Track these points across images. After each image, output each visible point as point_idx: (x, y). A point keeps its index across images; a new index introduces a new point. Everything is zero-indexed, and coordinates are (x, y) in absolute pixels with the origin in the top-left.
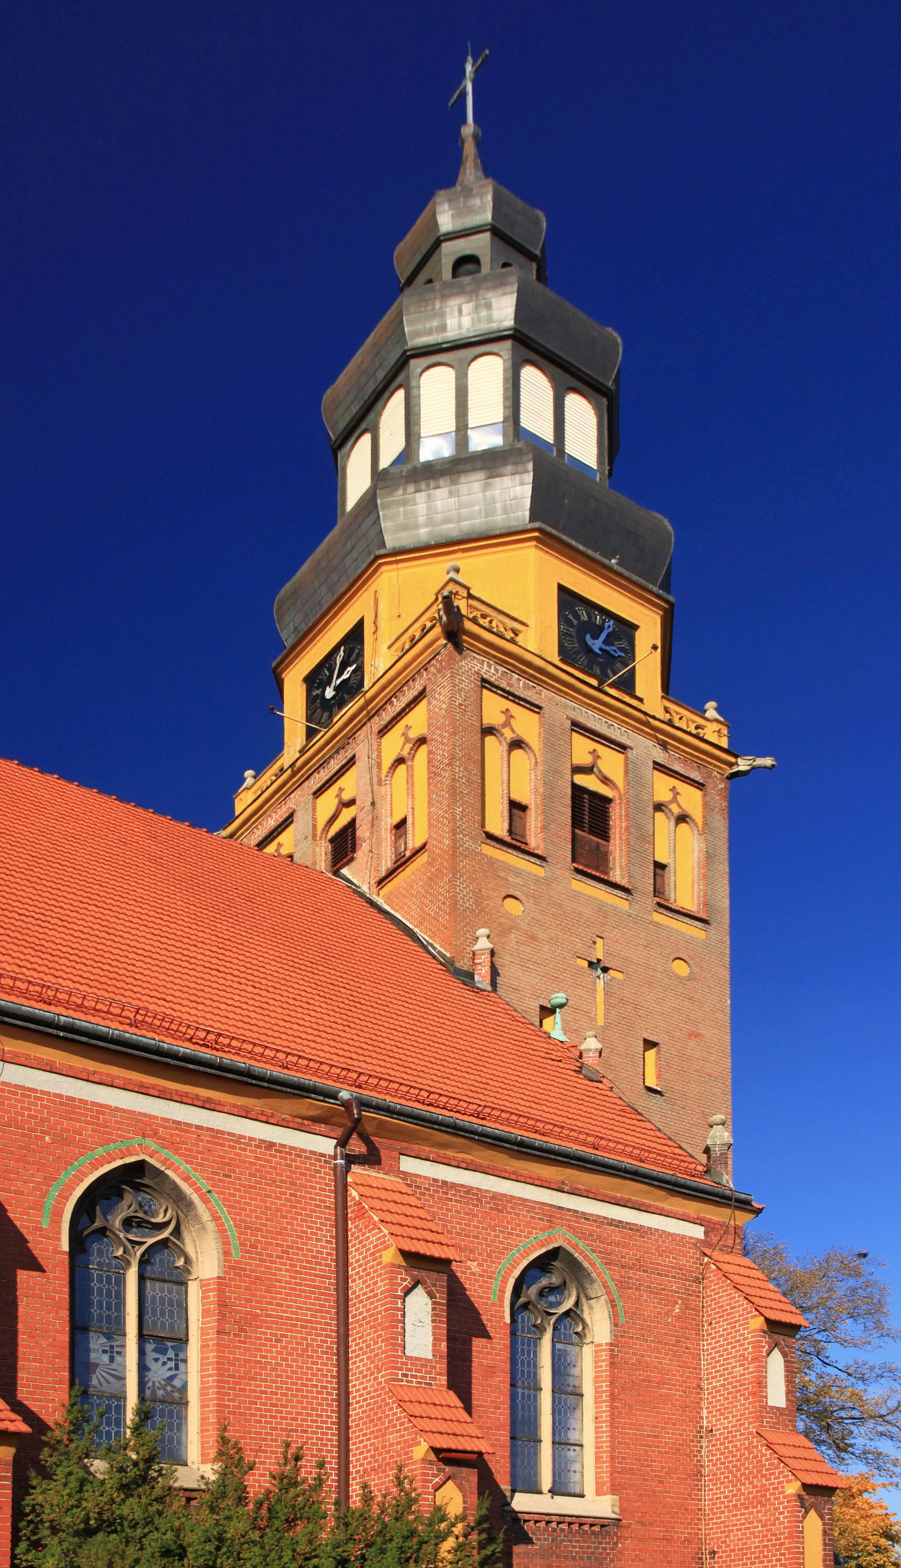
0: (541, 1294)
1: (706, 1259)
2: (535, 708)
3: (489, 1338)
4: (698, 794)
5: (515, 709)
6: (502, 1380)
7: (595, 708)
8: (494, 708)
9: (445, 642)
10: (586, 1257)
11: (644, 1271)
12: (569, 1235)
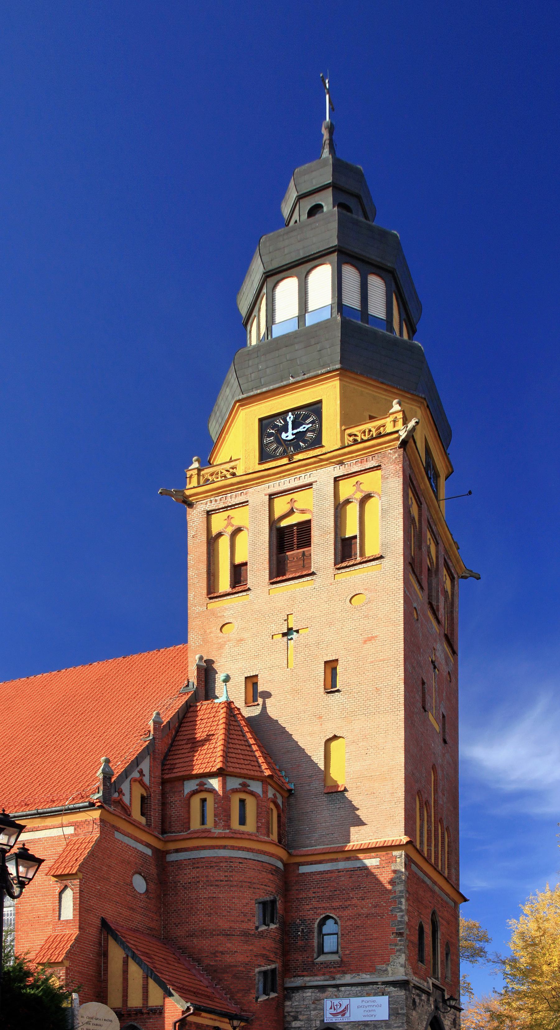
4: (379, 472)
7: (284, 476)
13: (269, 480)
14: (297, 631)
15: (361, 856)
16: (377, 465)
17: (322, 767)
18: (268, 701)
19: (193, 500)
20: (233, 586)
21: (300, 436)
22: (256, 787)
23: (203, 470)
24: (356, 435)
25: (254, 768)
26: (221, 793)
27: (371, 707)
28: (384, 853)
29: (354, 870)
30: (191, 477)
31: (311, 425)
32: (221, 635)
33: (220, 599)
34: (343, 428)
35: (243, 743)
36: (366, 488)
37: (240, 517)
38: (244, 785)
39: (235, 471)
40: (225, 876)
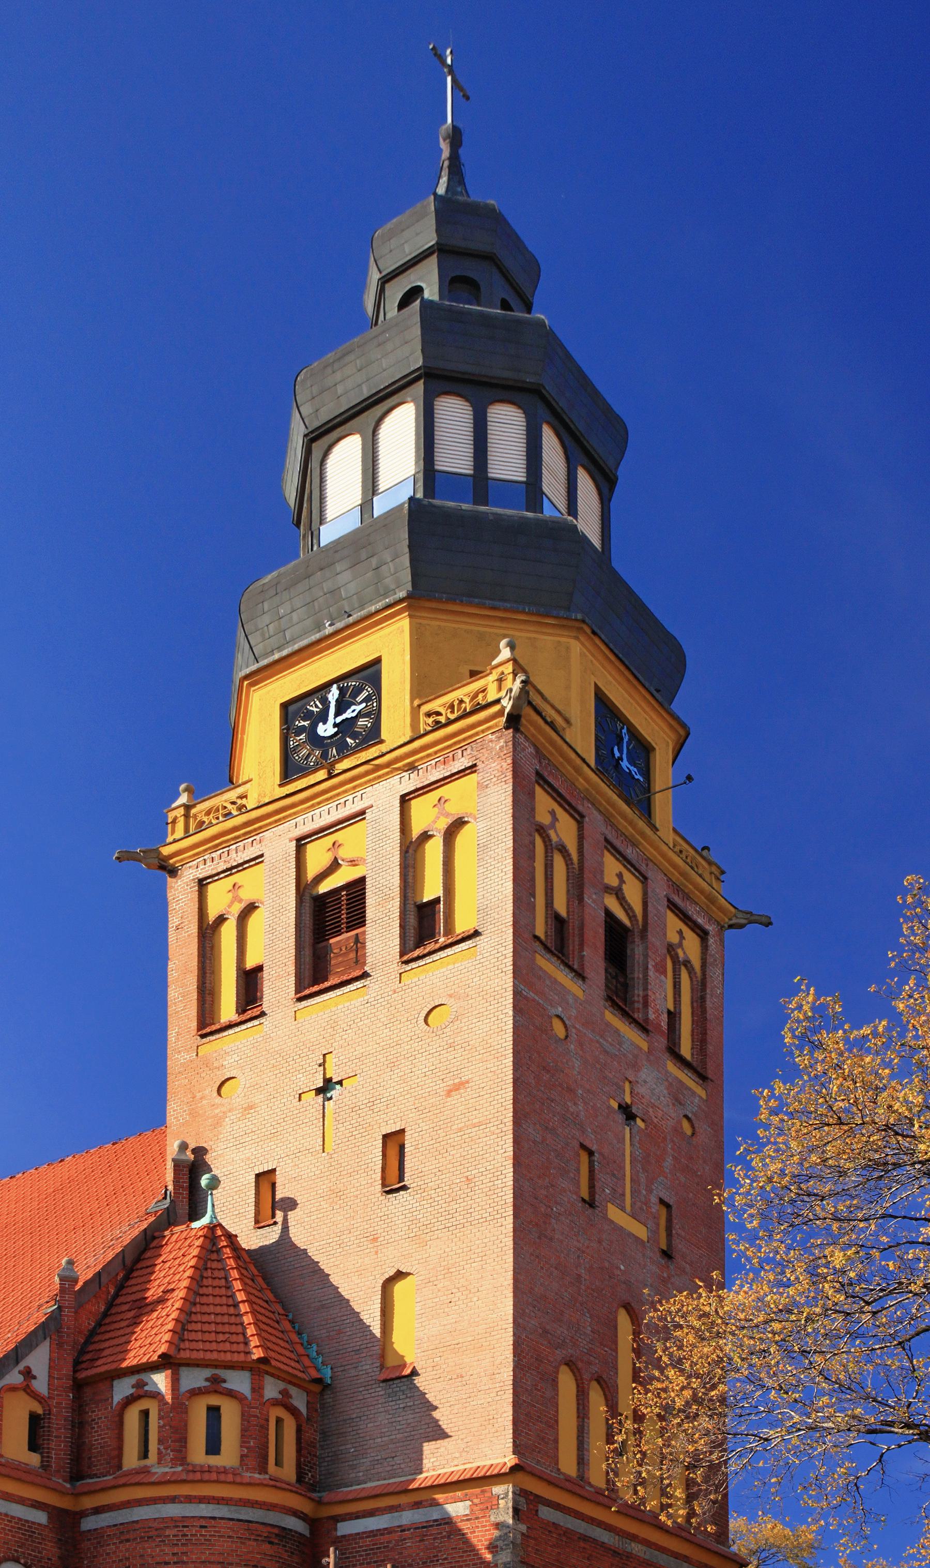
13: (295, 813)
14: (340, 1083)
15: (440, 1497)
16: (470, 764)
17: (377, 1332)
18: (291, 1214)
19: (175, 863)
20: (241, 1010)
21: (345, 728)
22: (240, 1382)
23: (194, 806)
24: (438, 714)
25: (235, 1347)
26: (169, 1398)
27: (457, 1214)
28: (478, 1490)
29: (427, 1526)
30: (174, 822)
31: (364, 705)
32: (218, 1100)
33: (217, 1036)
34: (416, 703)
35: (224, 1300)
36: (454, 809)
37: (252, 884)
38: (216, 1381)
39: (244, 801)
40: (174, 1554)
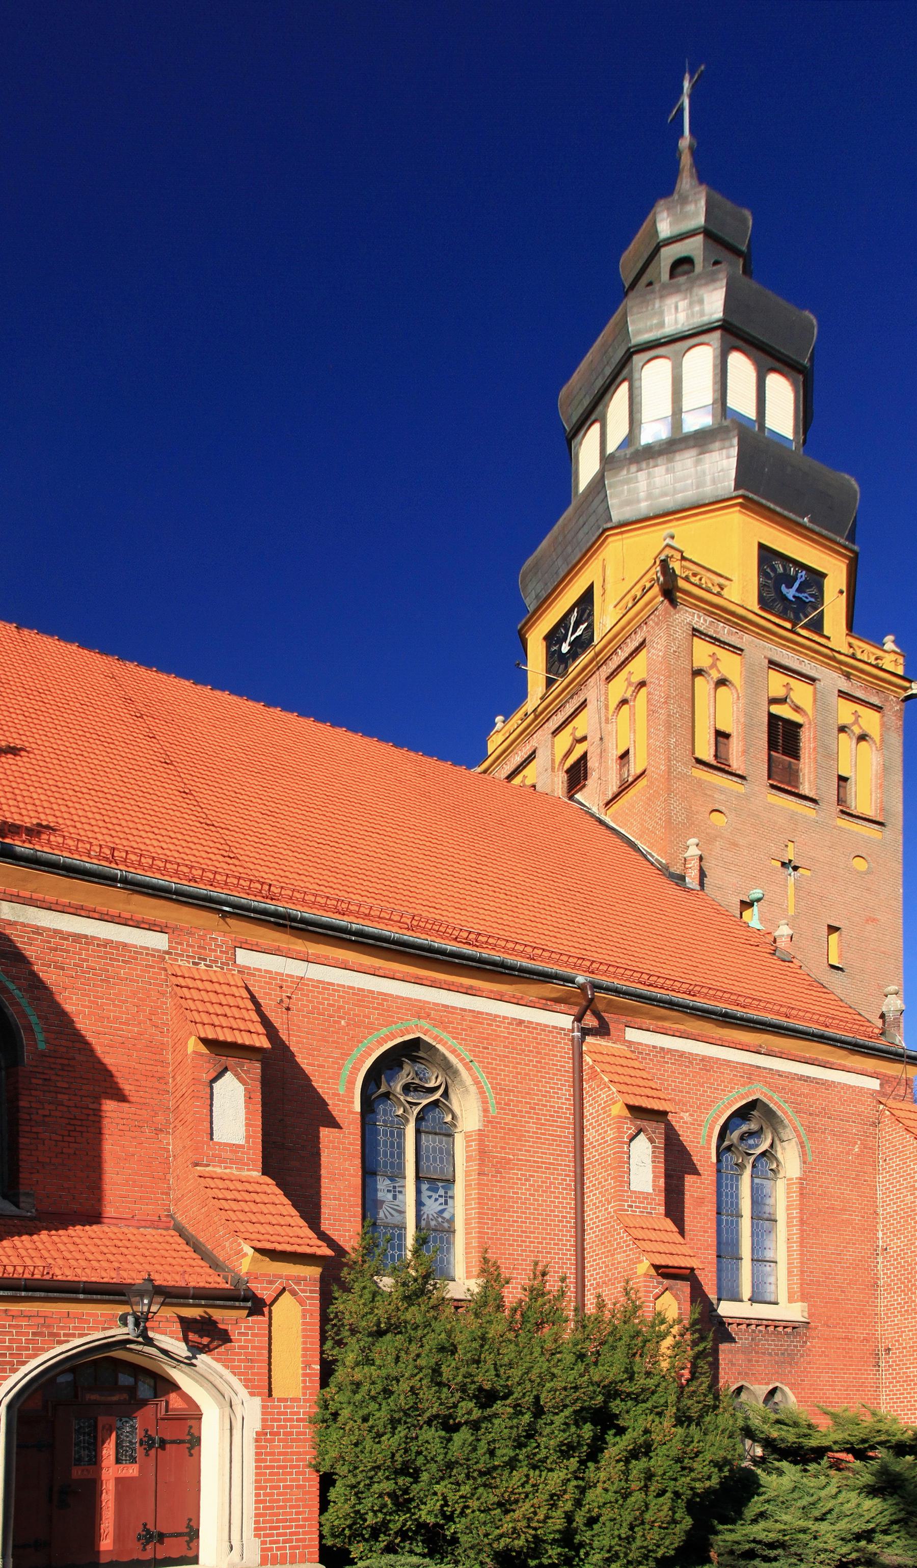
0: (742, 1138)
1: (882, 1107)
2: (737, 650)
3: (699, 1174)
4: (877, 715)
5: (721, 653)
6: (710, 1209)
7: (789, 647)
8: (702, 652)
9: (662, 599)
10: (779, 1107)
11: (829, 1118)
12: (765, 1089)
31: (813, 600)
